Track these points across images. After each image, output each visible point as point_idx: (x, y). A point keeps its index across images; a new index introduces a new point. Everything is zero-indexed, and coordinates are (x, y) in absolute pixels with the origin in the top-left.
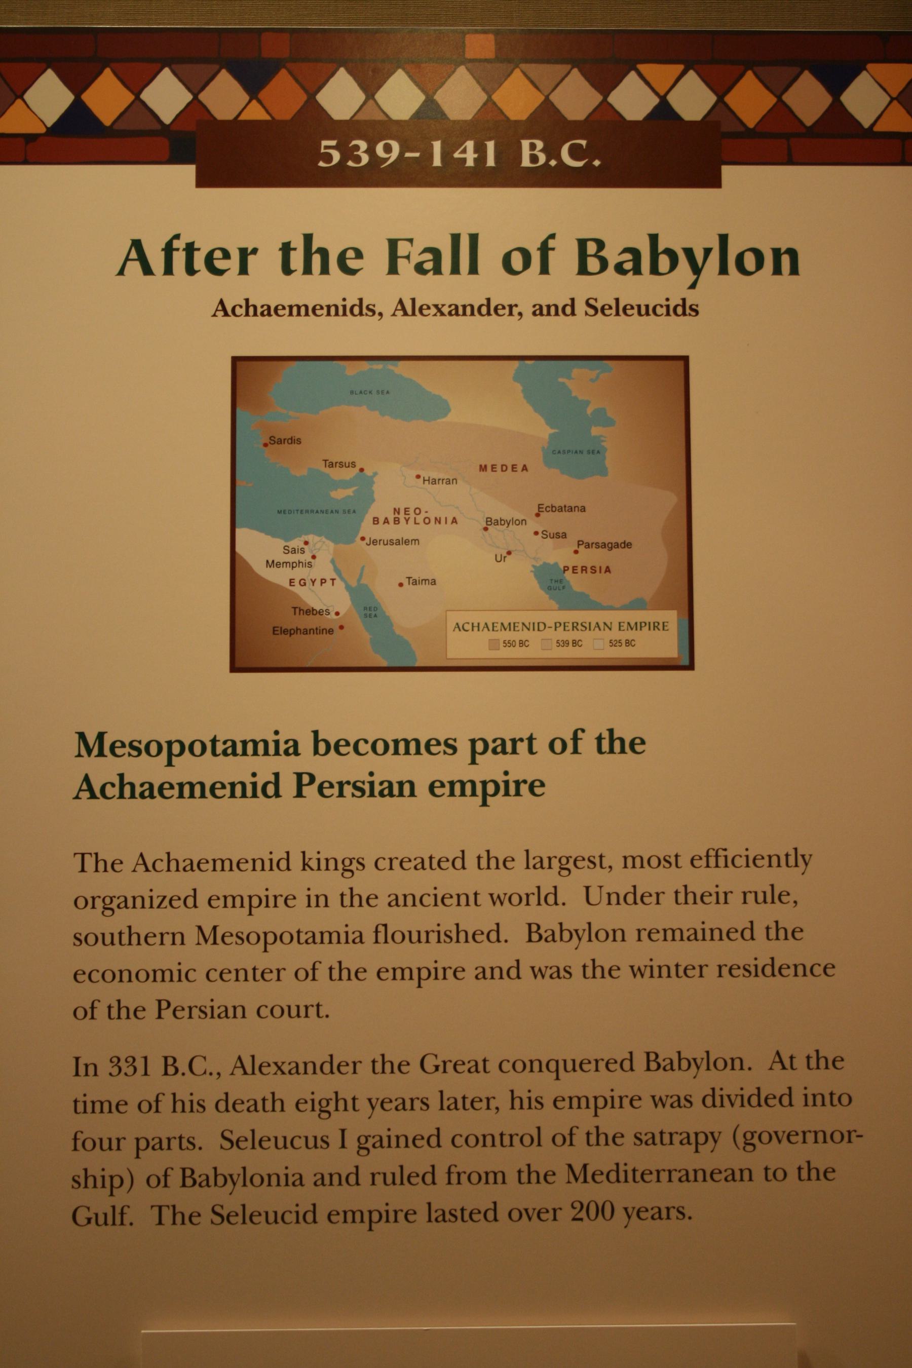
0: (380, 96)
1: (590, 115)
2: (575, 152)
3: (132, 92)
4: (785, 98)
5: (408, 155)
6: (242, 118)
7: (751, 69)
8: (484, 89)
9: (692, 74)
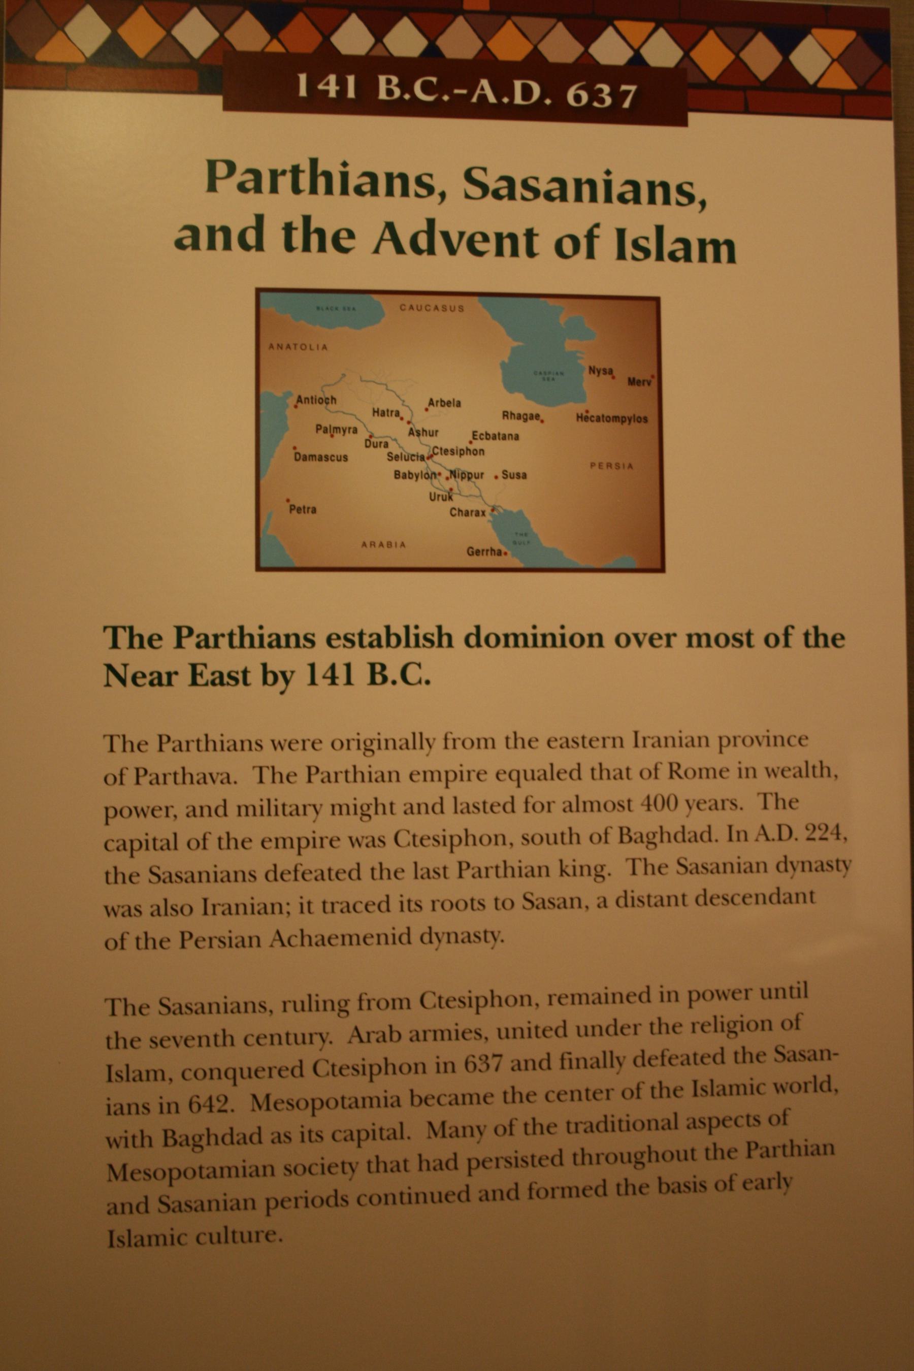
3: (164, 28)
8: (480, 37)
9: (661, 32)
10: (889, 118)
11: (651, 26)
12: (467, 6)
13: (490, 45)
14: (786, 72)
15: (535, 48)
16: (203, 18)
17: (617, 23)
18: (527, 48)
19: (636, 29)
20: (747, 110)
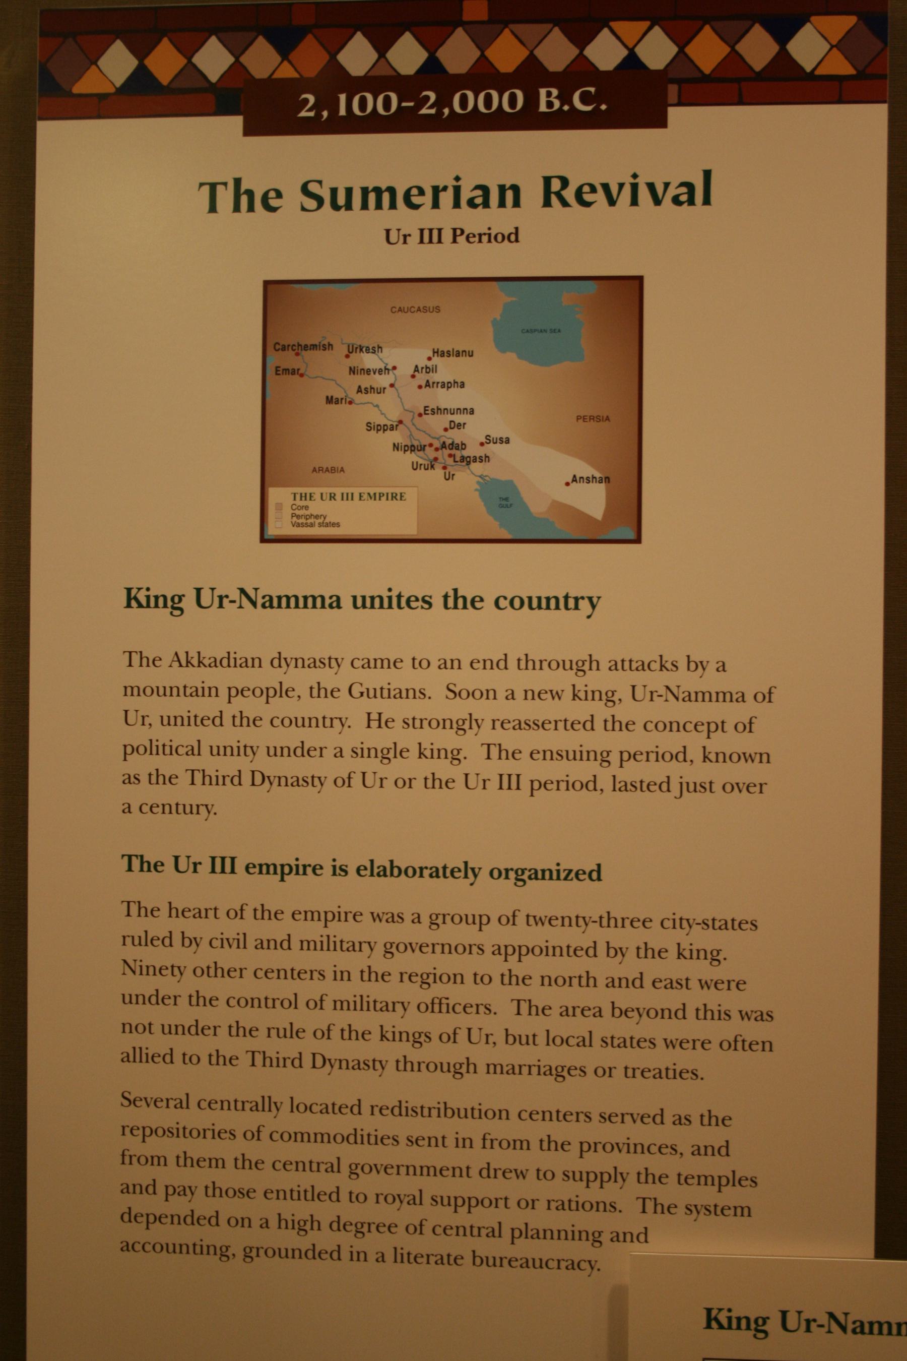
0: (391, 55)
2: (585, 99)
4: (738, 47)
7: (709, 23)
9: (657, 30)
10: (884, 102)
11: (646, 24)
12: (466, 17)
19: (629, 29)
20: (741, 101)
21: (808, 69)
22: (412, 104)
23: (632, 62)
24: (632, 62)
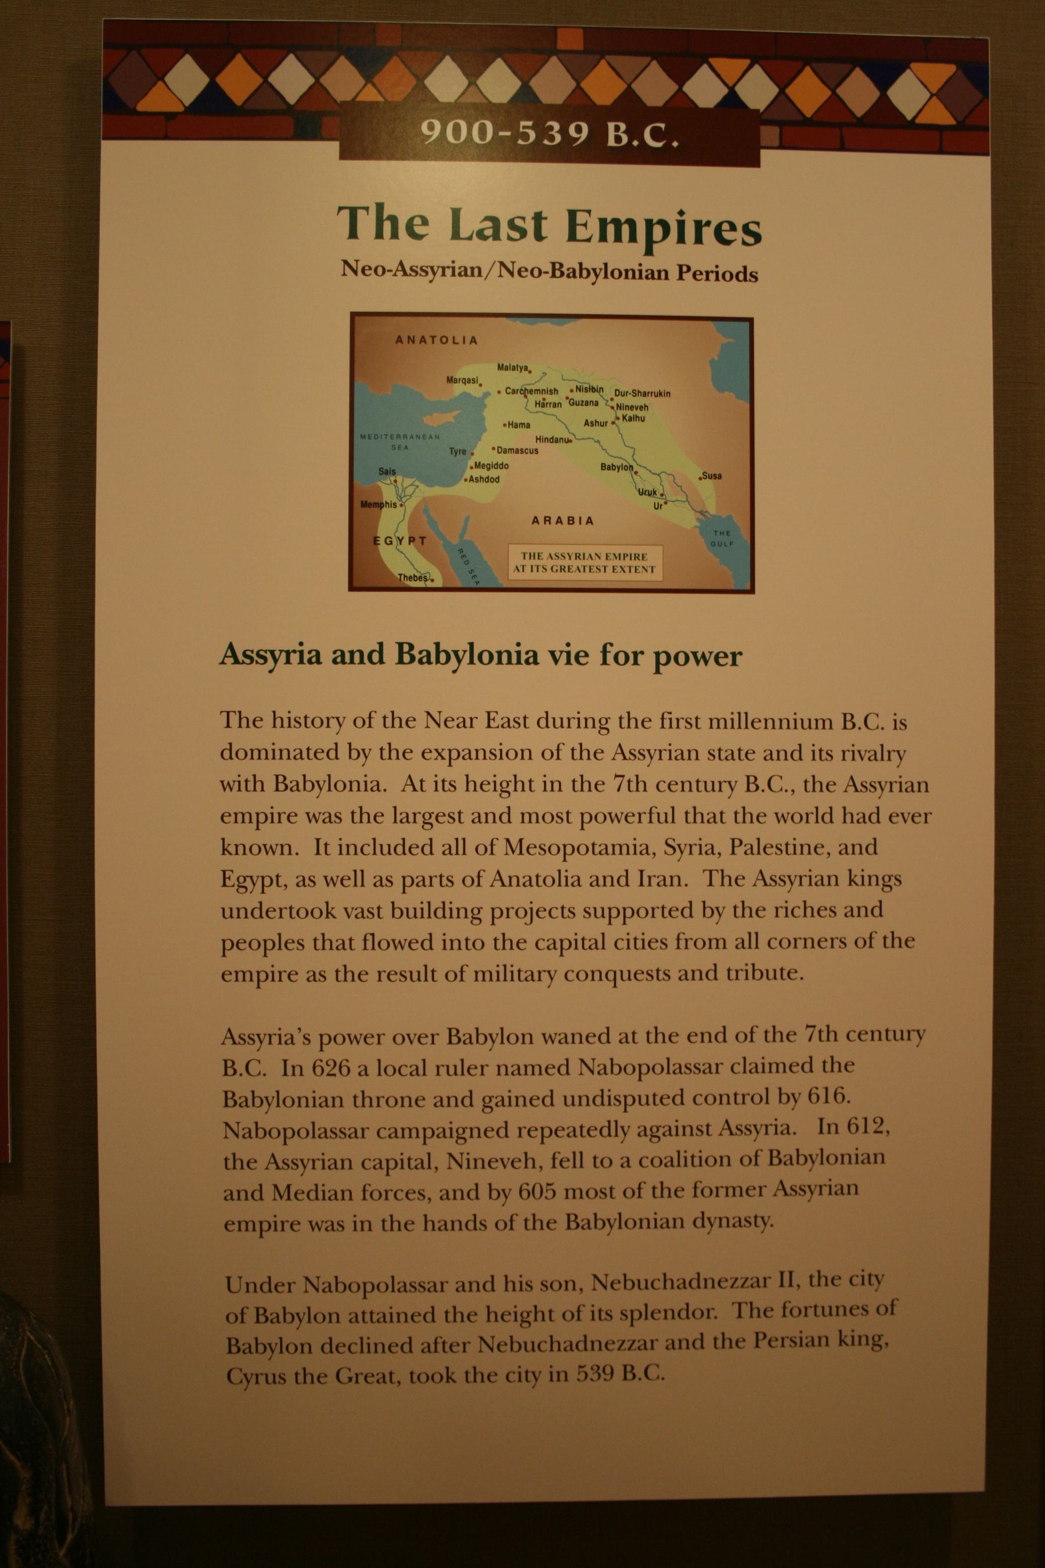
1: (667, 103)
4: (839, 91)
5: (501, 134)
6: (359, 99)
8: (573, 77)
9: (757, 69)
10: (987, 154)
13: (583, 85)
14: (884, 108)
15: (629, 86)
16: (299, 65)
17: (712, 61)
18: (622, 87)
20: (842, 147)
21: (909, 117)
22: (508, 134)
23: (732, 101)
24: (732, 101)
